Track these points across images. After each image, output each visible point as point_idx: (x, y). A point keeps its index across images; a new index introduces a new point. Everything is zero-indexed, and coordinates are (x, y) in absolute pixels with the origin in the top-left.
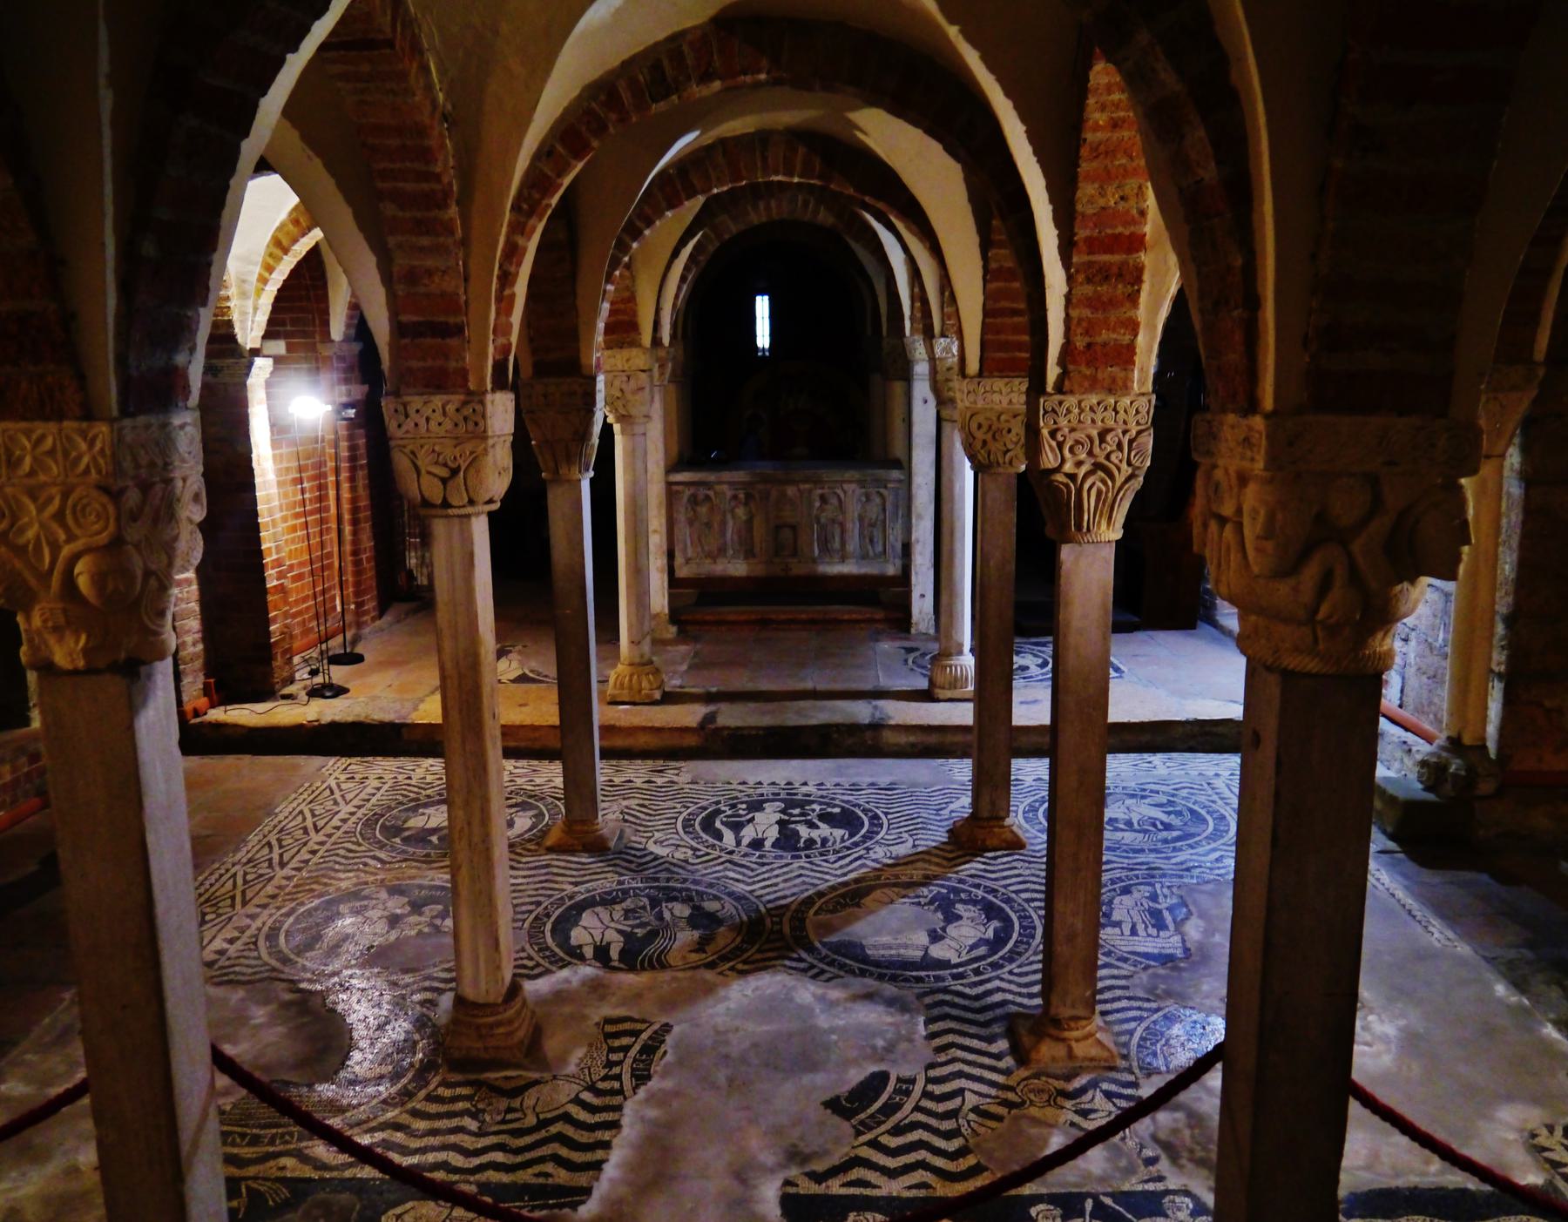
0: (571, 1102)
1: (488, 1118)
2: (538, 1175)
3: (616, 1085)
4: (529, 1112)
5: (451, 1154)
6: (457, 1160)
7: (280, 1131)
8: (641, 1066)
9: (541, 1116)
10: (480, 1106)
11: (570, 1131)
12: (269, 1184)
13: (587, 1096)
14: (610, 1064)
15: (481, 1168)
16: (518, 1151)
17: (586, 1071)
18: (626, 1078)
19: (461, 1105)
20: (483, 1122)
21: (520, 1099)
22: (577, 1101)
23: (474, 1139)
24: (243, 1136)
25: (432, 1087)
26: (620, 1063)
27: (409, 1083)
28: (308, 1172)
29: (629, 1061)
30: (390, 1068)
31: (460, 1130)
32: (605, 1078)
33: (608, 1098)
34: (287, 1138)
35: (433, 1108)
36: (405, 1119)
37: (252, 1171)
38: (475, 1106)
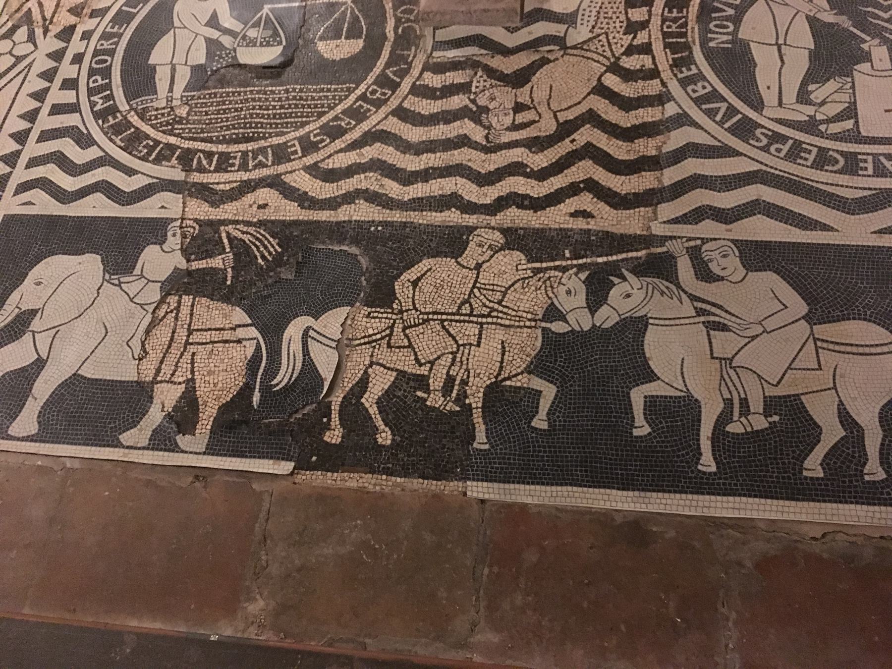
0: (594, 91)
1: (494, 121)
2: (575, 214)
3: (647, 61)
4: (543, 109)
5: (461, 181)
6: (470, 192)
7: (250, 146)
8: (674, 29)
9: (562, 117)
10: (482, 101)
11: (603, 141)
12: (251, 230)
13: (612, 81)
14: (633, 28)
15: (501, 204)
16: (542, 175)
17: (603, 38)
18: (658, 47)
19: (457, 102)
20: (489, 127)
21: (527, 87)
22: (601, 90)
23: (483, 156)
24: (209, 155)
25: (415, 72)
26: (644, 25)
27: (388, 65)
28: (291, 211)
29: (656, 22)
30: (361, 43)
31: (463, 141)
32: (630, 51)
33: (641, 83)
34: (260, 157)
35: (426, 107)
36: (394, 125)
37: (227, 211)
38: (473, 101)
